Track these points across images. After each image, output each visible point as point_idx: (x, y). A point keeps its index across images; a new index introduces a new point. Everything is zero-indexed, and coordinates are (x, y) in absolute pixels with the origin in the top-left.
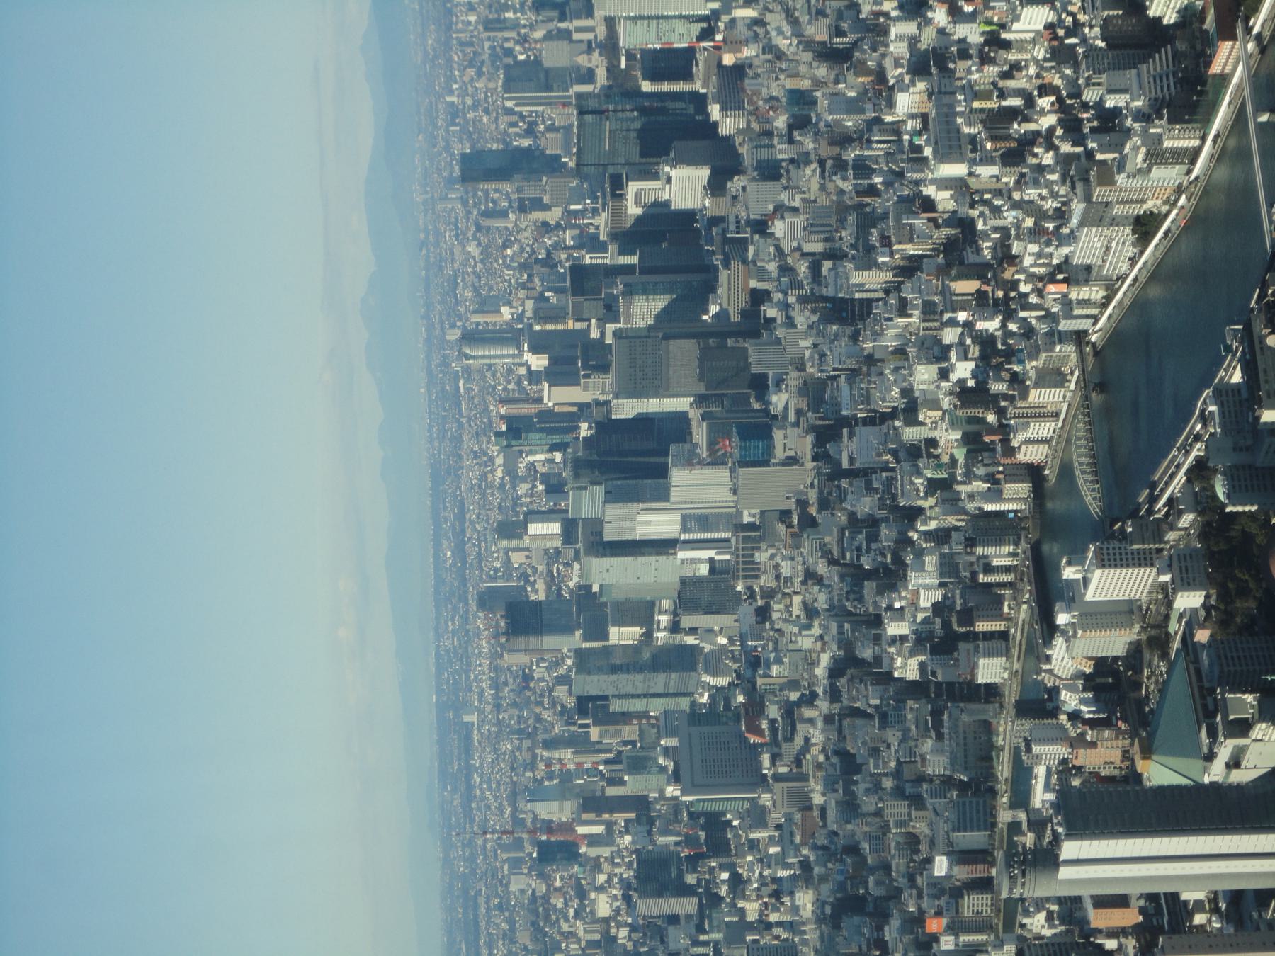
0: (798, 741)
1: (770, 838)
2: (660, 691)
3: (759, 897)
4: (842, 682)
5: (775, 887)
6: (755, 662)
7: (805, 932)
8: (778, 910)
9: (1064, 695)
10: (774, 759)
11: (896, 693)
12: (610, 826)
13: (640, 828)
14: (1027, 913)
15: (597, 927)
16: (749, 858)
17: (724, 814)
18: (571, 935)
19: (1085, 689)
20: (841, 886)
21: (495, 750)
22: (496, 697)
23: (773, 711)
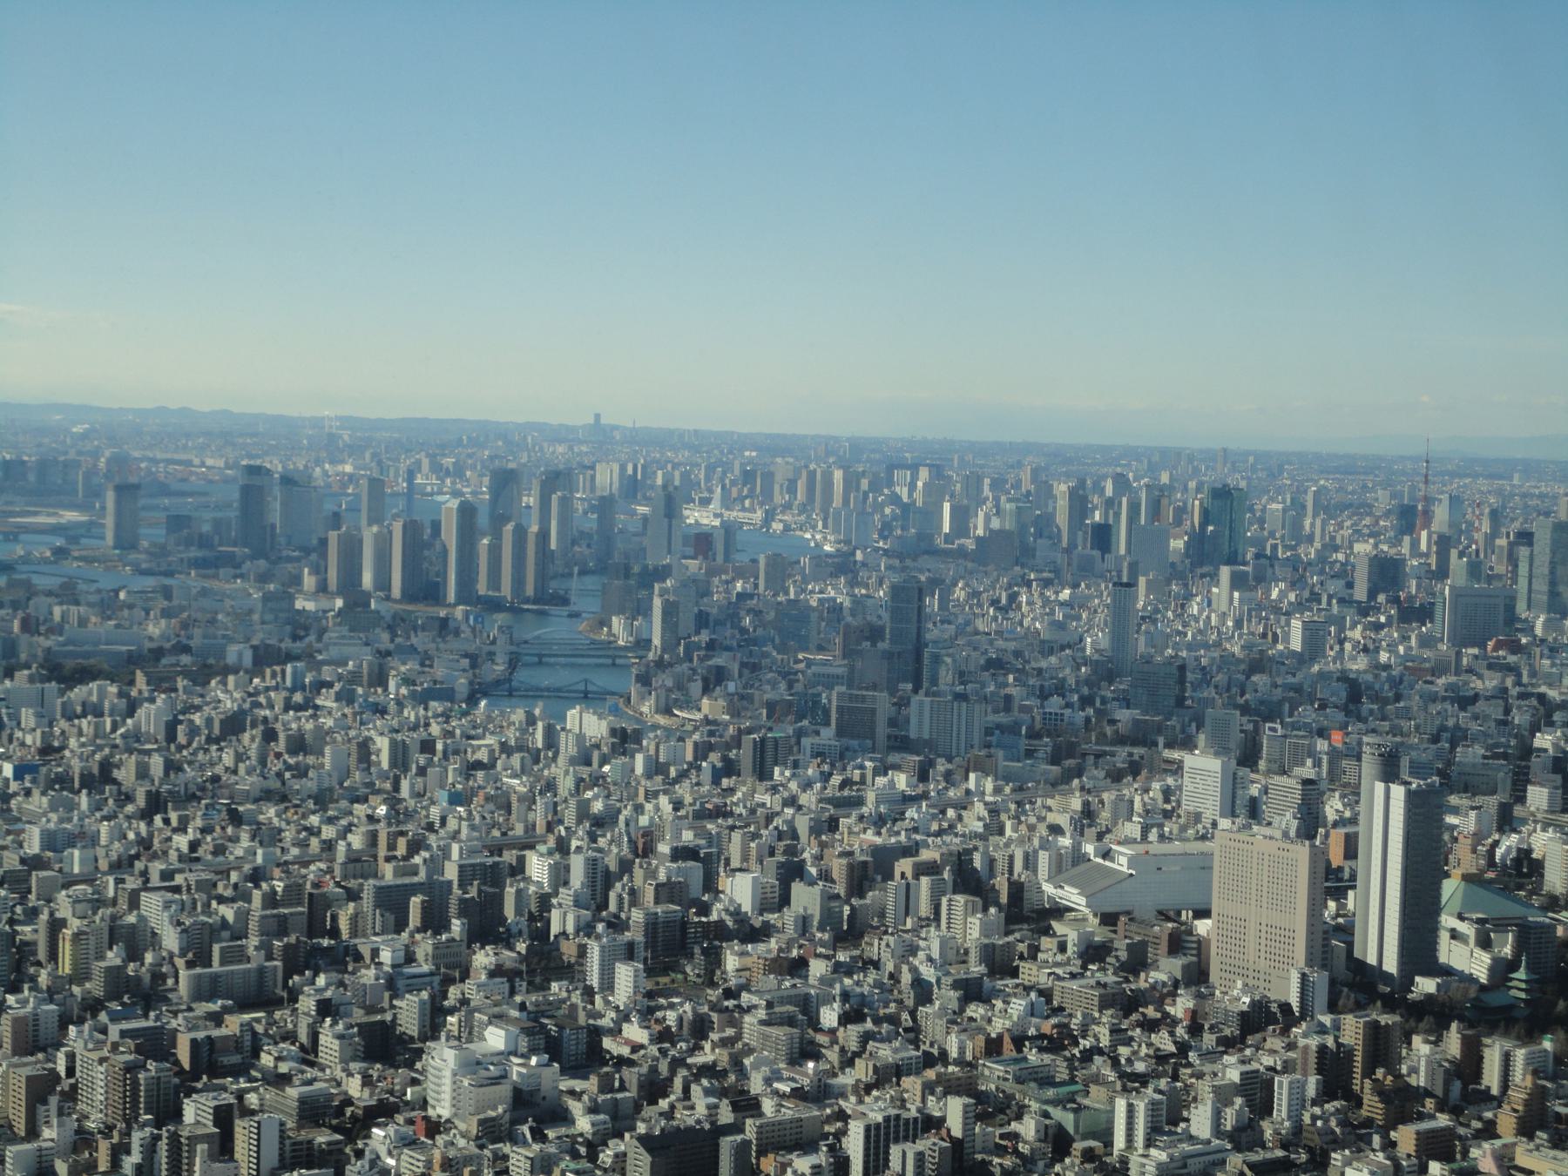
0: (1486, 673)
1: (1411, 648)
2: (1535, 587)
3: (1364, 638)
4: (1534, 702)
5: (1372, 647)
6: (1553, 651)
7: (1335, 663)
8: (1353, 649)
9: (1514, 837)
10: (1476, 657)
11: (1522, 736)
12: (1427, 555)
13: (1423, 571)
14: (1343, 796)
15: (1346, 543)
16: (1396, 635)
17: (1432, 622)
18: (1340, 526)
19: (1519, 850)
20: (1370, 687)
21: (1490, 492)
22: (1532, 495)
23: (1512, 659)
